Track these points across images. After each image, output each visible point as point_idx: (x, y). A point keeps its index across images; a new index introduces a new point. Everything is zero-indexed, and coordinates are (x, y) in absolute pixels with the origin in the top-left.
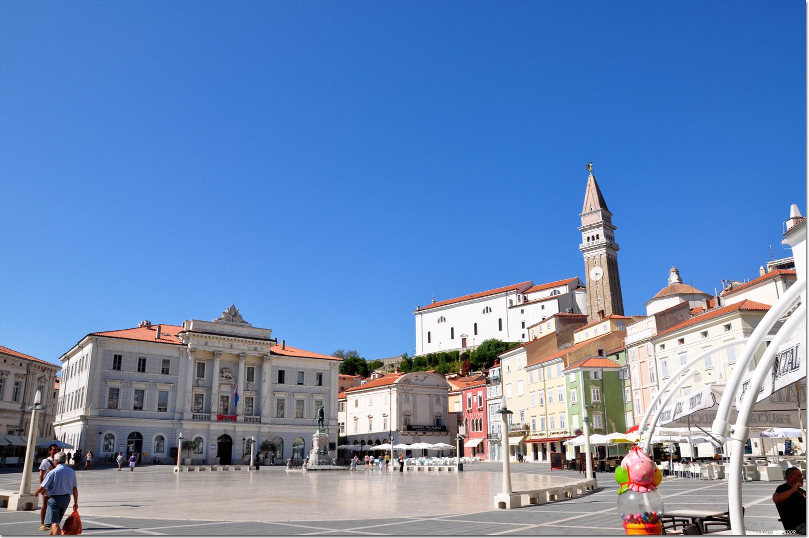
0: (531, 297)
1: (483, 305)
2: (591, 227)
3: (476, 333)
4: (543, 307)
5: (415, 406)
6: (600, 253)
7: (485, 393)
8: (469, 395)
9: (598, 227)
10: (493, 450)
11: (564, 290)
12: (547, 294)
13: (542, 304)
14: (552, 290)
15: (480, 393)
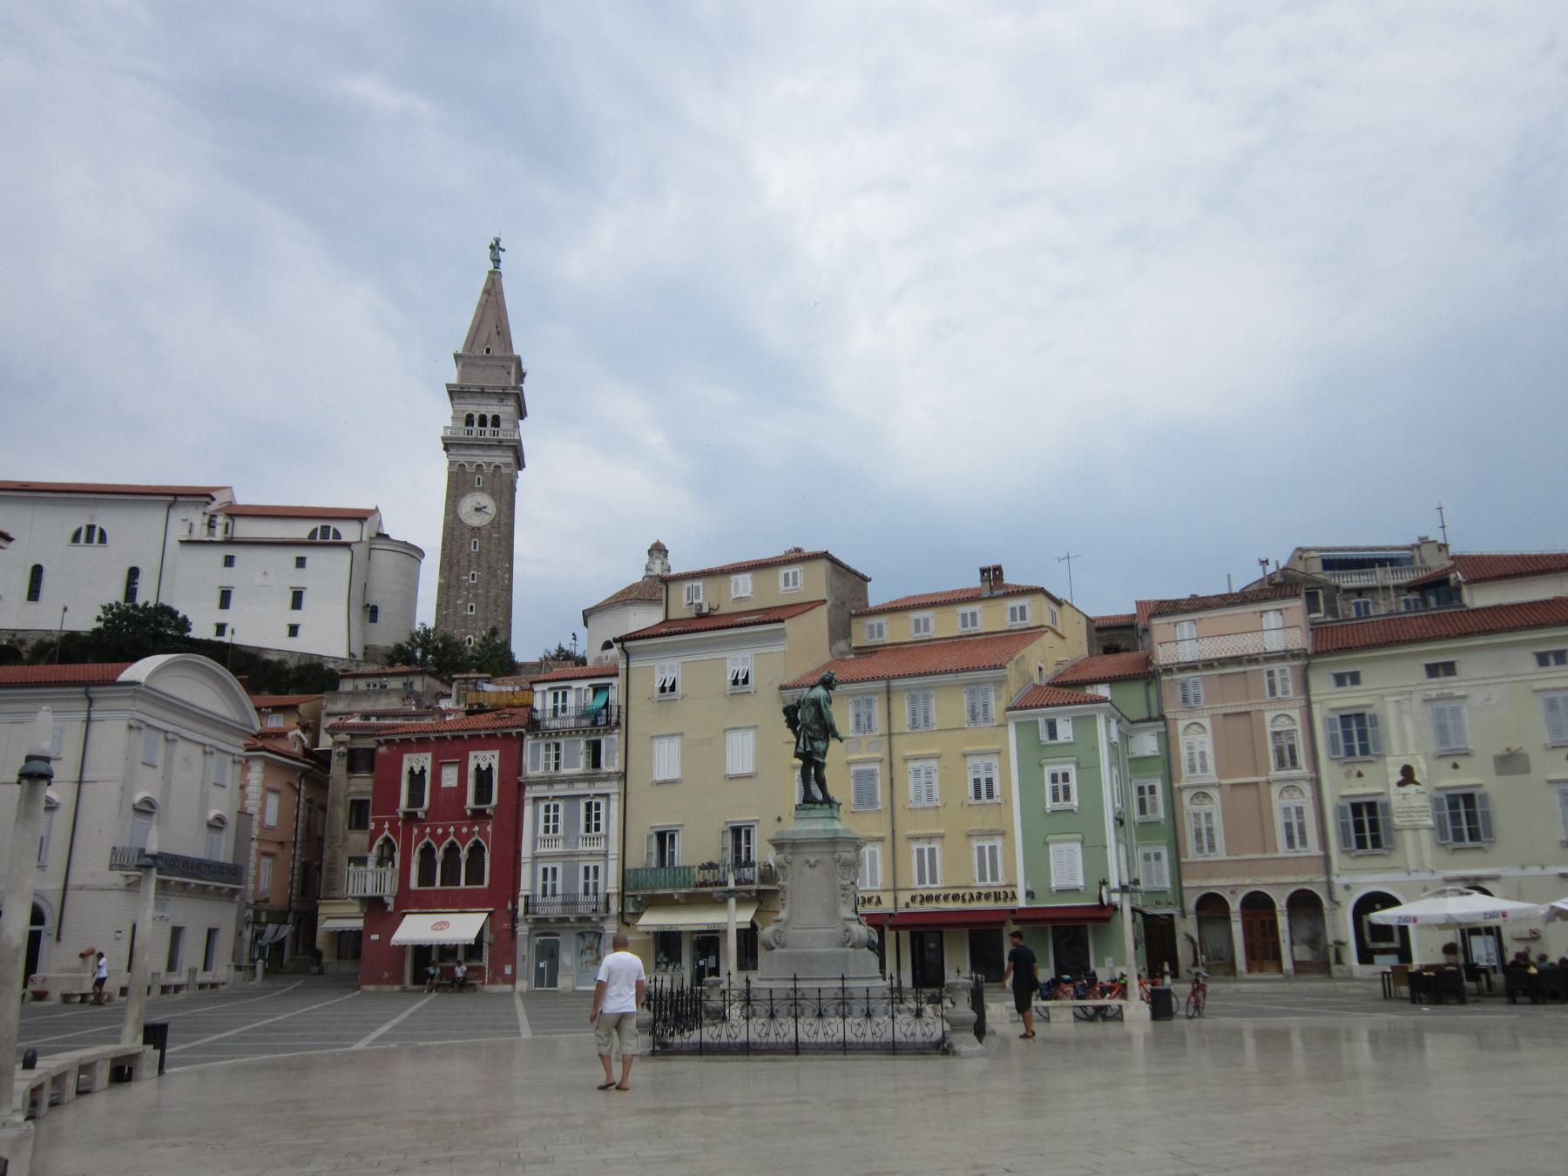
0: (244, 529)
1: (79, 518)
2: (482, 392)
3: (34, 593)
4: (301, 562)
5: (166, 780)
6: (498, 461)
7: (513, 764)
8: (420, 761)
9: (503, 395)
10: (549, 953)
11: (349, 532)
12: (302, 530)
13: (301, 552)
14: (318, 524)
15: (488, 758)
